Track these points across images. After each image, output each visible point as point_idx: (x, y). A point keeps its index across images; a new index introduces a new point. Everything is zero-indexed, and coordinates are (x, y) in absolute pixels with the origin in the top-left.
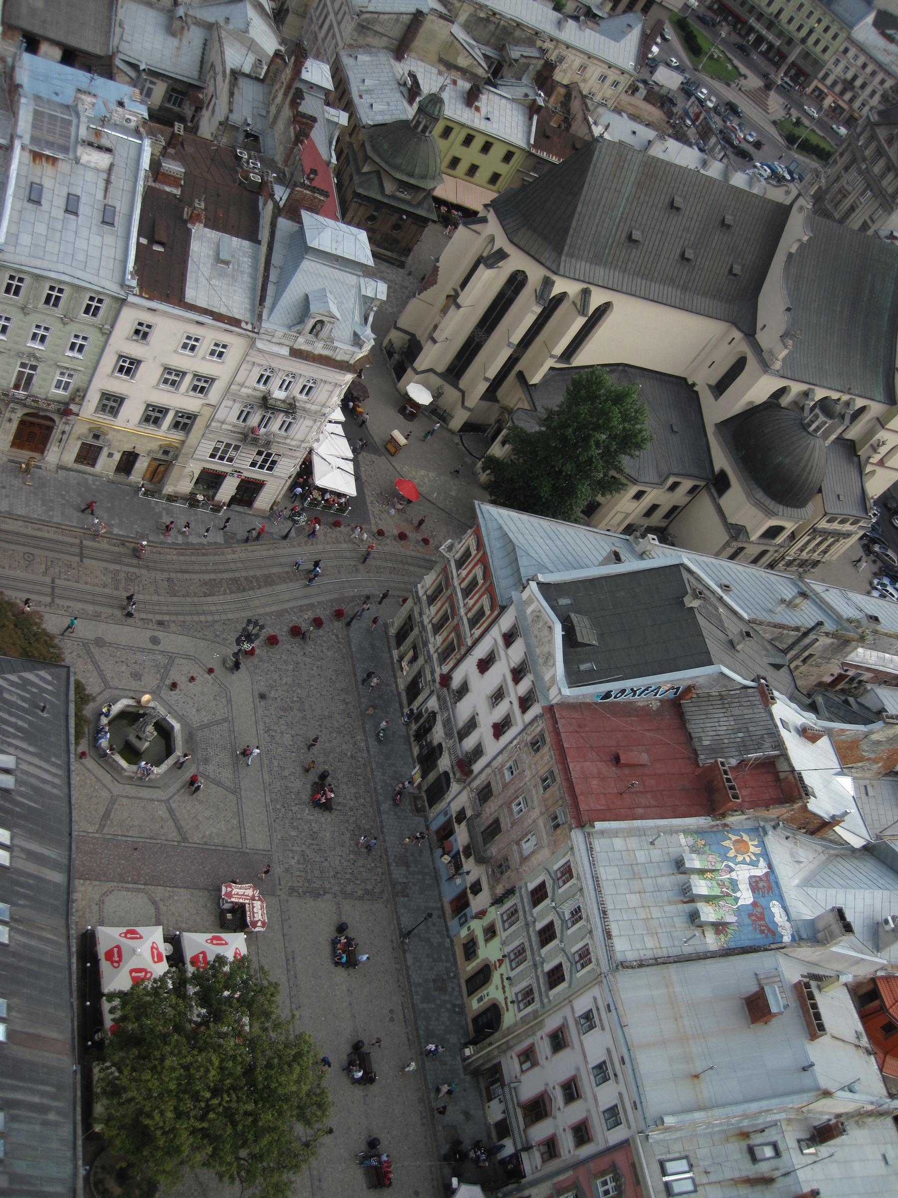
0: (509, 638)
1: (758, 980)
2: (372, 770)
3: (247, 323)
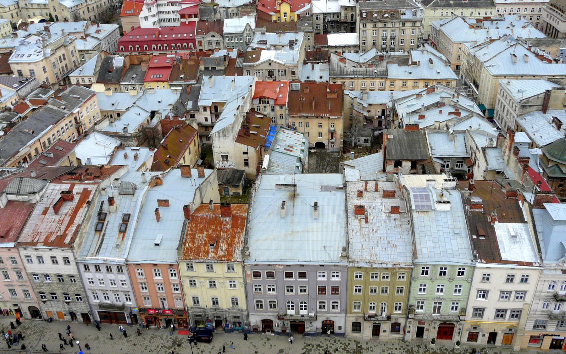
3: (535, 263)
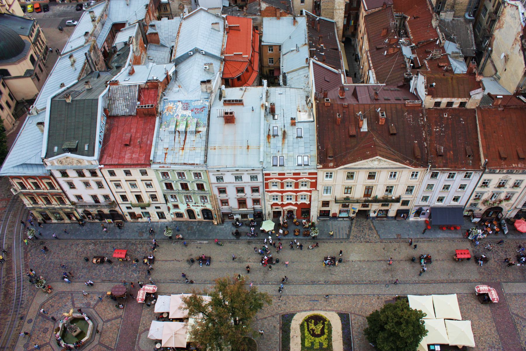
0: (64, 174)
1: (220, 117)
2: (102, 239)
